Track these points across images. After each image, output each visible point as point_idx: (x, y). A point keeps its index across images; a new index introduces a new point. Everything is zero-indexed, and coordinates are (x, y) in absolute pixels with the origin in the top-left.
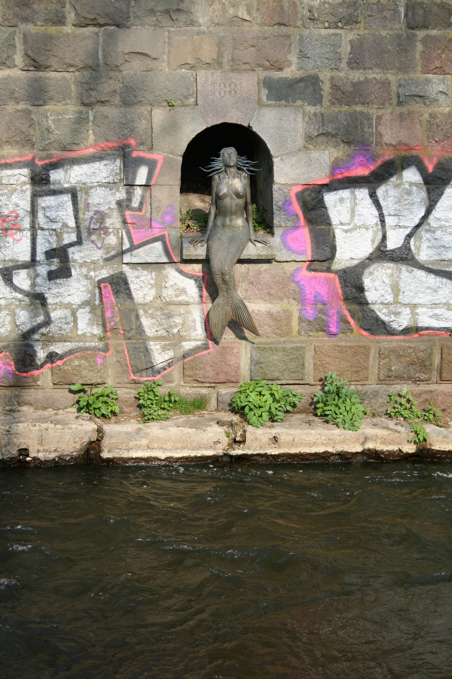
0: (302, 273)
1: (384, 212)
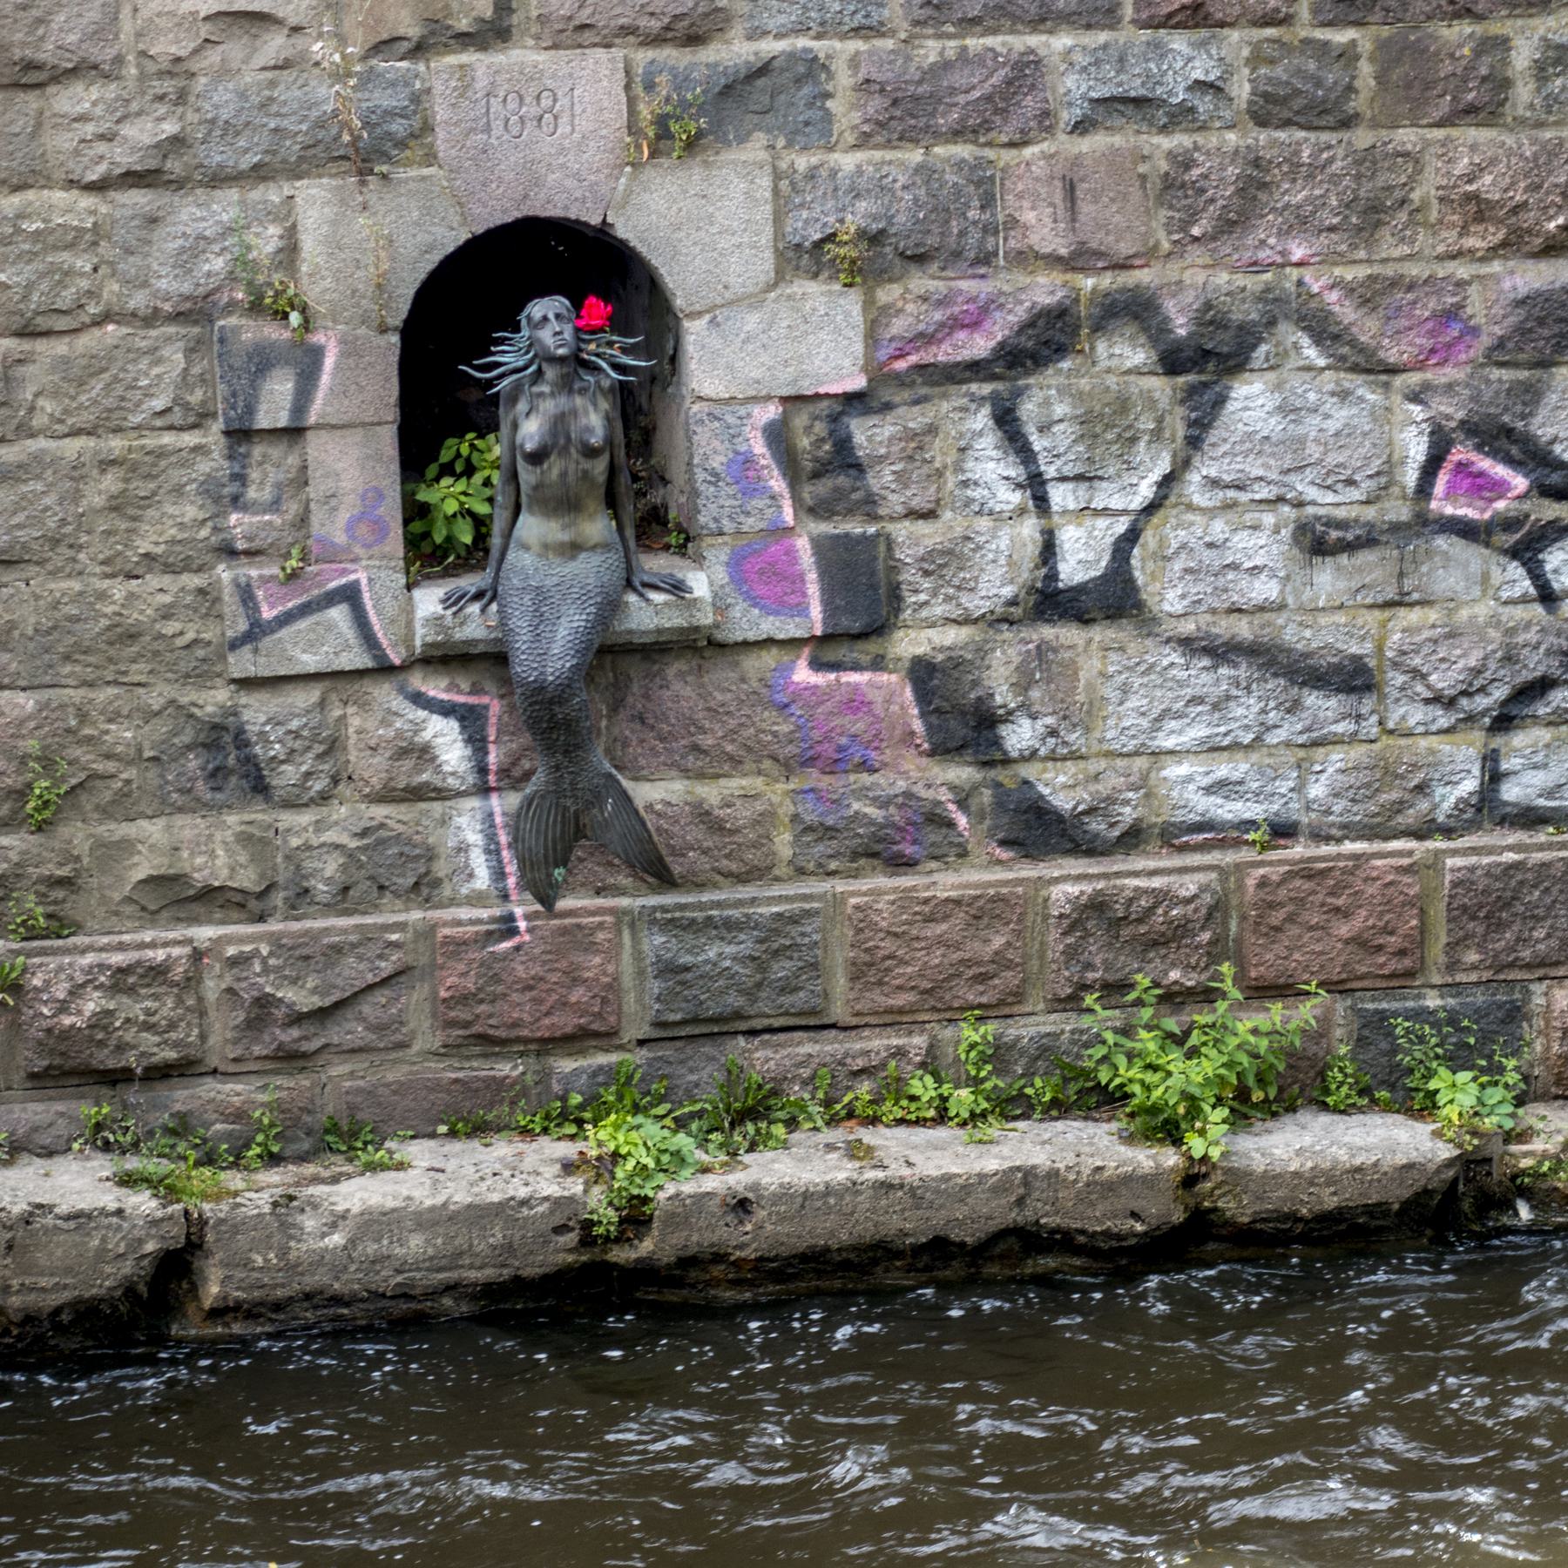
0: (796, 678)
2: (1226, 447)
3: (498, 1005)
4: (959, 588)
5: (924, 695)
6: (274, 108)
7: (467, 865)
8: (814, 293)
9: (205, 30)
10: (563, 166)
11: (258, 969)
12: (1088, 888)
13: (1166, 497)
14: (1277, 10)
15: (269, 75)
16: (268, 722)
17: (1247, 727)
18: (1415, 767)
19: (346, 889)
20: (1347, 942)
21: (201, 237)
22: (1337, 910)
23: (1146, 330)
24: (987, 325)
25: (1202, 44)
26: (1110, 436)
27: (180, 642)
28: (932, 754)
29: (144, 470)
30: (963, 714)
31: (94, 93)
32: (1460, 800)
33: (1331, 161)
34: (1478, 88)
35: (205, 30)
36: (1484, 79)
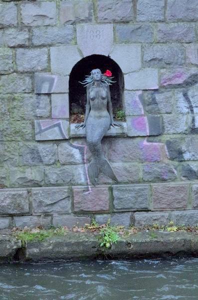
0: (144, 143)
1: (193, 105)
5: (169, 147)
8: (149, 70)
21: (32, 57)
28: (170, 159)
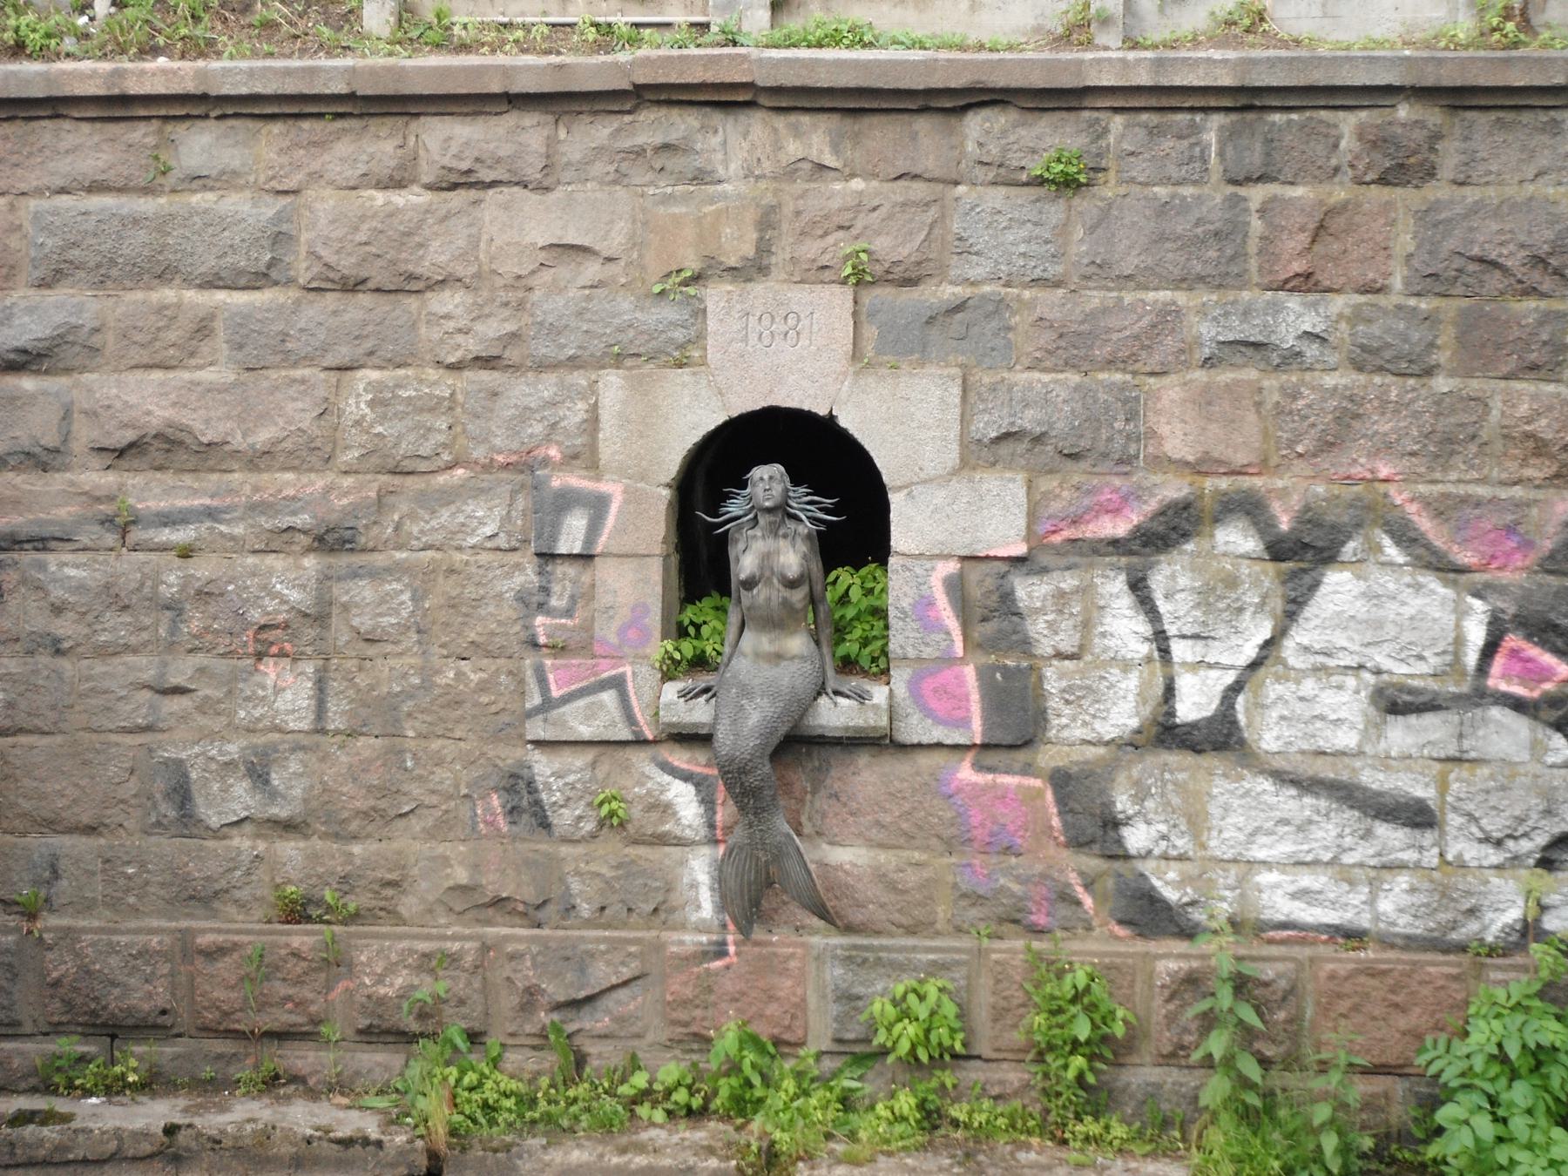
1: (1166, 627)
2: (1317, 622)
3: (710, 1013)
4: (1094, 716)
5: (1061, 801)
6: (588, 316)
7: (697, 899)
8: (990, 482)
9: (542, 256)
10: (801, 370)
11: (529, 964)
12: (1184, 965)
13: (1266, 657)
14: (1375, 281)
15: (587, 292)
16: (553, 774)
17: (1326, 848)
18: (1469, 893)
19: (603, 909)
20: (1404, 1034)
21: (527, 408)
22: (1396, 1006)
23: (1255, 524)
24: (1126, 511)
25: (1314, 305)
26: (1221, 605)
27: (493, 709)
28: (1067, 845)
29: (477, 579)
30: (1093, 815)
31: (458, 298)
32: (1506, 925)
33: (1412, 401)
34: (1539, 350)
35: (542, 256)
36: (1545, 343)
